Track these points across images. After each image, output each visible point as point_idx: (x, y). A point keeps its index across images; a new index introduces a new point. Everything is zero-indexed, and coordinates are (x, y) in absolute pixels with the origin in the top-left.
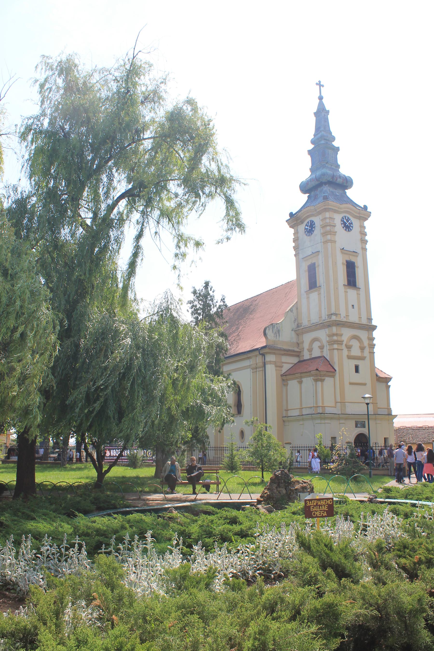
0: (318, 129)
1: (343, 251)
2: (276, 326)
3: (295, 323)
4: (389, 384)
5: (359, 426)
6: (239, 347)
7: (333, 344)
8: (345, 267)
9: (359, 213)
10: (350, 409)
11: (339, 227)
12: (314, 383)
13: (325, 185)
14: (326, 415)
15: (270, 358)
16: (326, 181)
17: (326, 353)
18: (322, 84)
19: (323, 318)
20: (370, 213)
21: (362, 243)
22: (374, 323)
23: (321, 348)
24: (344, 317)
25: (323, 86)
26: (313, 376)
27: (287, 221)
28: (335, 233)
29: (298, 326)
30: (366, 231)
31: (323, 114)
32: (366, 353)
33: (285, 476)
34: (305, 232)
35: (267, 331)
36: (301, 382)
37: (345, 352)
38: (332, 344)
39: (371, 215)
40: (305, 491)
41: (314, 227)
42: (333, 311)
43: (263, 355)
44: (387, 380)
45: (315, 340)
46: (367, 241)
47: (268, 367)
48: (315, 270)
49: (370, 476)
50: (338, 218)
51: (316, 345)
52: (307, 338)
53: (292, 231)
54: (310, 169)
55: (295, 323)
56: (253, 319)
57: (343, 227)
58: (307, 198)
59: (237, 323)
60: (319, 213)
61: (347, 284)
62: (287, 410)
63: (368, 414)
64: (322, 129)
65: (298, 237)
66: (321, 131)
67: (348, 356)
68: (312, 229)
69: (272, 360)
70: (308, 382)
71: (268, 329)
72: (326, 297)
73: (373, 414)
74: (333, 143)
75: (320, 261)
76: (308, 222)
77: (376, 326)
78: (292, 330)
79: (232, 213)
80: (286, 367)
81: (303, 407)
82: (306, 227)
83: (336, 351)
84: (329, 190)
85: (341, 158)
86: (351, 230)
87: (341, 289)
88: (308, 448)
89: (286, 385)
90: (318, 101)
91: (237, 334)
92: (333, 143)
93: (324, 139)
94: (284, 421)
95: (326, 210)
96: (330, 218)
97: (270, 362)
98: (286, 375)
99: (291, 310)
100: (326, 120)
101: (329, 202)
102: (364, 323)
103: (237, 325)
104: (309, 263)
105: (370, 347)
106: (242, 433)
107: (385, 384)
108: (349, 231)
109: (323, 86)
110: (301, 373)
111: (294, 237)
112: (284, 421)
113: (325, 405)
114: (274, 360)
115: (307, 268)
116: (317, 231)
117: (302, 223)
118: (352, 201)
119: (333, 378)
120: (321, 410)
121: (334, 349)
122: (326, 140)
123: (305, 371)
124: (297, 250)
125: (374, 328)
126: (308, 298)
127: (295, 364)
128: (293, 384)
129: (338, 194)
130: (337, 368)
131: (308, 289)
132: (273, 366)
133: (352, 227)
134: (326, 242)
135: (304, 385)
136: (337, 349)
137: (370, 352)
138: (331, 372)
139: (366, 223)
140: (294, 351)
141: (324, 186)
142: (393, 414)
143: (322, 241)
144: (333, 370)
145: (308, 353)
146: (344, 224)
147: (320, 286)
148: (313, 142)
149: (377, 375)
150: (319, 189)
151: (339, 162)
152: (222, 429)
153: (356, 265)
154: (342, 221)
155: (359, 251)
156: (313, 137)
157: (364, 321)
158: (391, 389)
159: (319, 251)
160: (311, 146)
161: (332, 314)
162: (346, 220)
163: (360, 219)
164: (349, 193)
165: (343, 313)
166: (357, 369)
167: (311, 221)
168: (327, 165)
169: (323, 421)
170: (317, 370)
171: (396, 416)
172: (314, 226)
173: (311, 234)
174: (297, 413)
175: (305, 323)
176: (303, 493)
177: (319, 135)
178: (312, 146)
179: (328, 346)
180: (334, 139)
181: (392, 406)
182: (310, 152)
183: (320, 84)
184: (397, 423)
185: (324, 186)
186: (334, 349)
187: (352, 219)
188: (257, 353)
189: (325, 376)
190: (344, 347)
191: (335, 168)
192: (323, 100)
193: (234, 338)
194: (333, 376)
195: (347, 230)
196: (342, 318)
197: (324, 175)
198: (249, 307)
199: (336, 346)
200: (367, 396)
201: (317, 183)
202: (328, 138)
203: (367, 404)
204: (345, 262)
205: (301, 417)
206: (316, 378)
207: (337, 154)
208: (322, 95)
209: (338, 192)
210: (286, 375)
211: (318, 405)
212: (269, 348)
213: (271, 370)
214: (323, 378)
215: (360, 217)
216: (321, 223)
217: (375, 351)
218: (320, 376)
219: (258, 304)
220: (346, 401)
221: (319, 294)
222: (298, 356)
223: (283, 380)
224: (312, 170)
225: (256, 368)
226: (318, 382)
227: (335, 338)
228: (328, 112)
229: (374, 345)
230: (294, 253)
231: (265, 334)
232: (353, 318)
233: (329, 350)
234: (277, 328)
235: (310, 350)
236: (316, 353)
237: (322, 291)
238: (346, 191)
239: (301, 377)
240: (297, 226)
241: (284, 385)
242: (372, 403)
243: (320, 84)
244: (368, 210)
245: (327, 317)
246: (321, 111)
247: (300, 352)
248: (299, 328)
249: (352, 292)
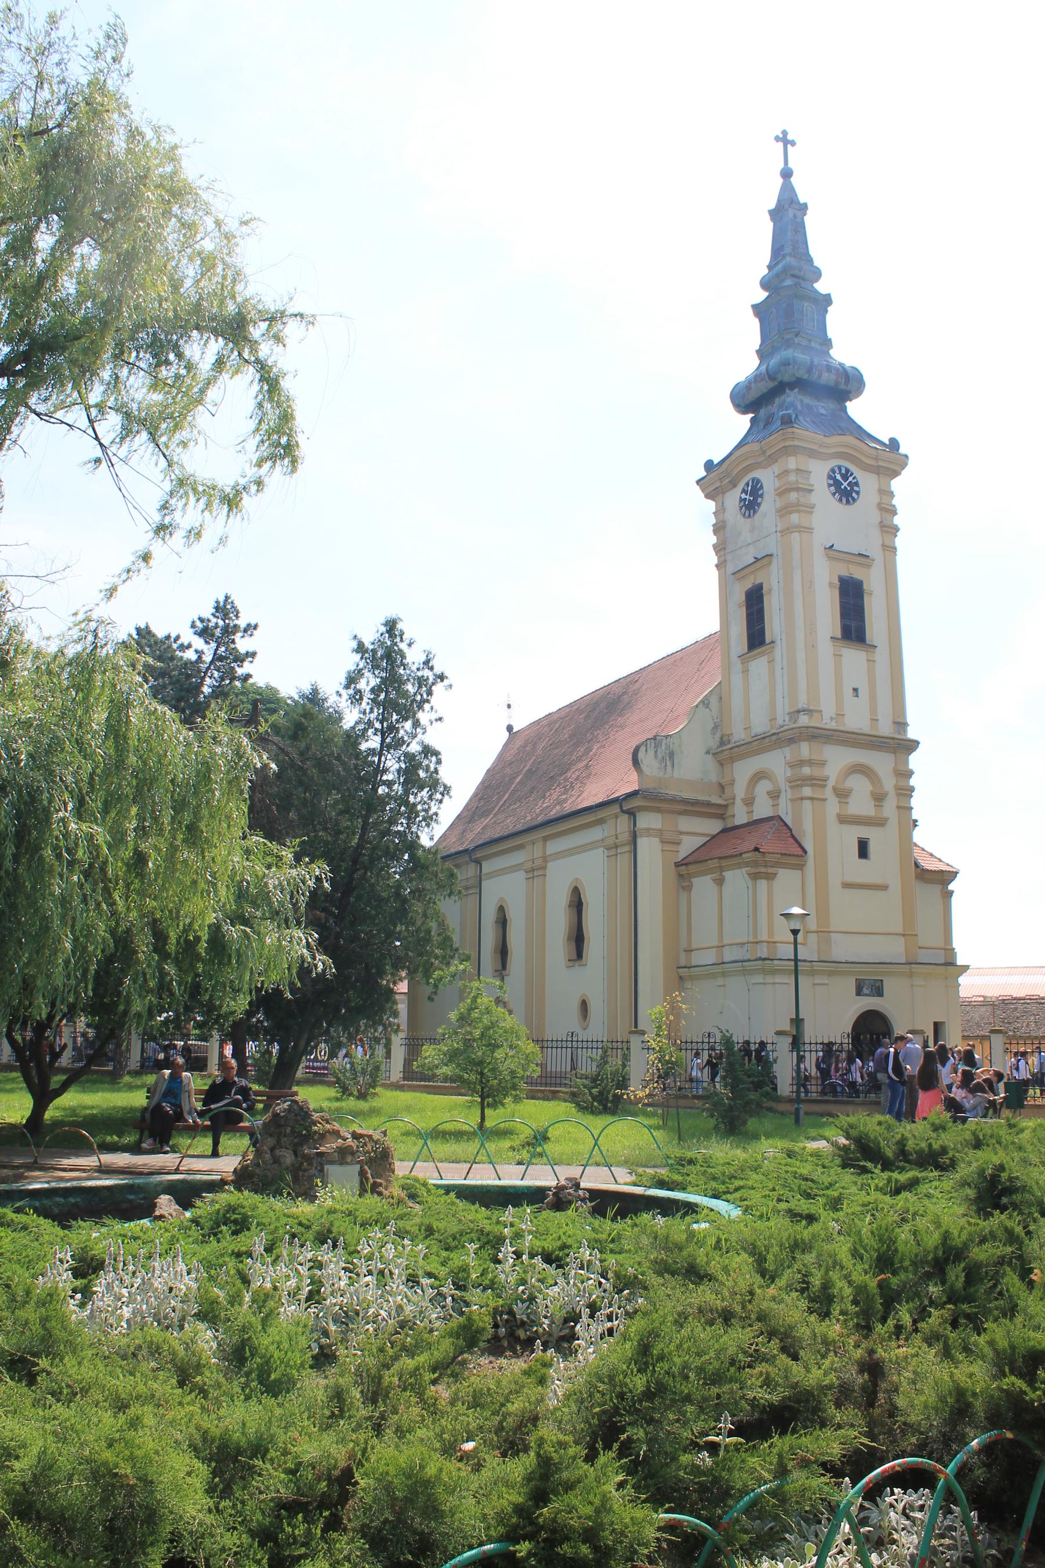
0: (777, 251)
1: (830, 553)
2: (664, 742)
3: (714, 734)
4: (951, 887)
5: (865, 991)
6: (584, 795)
7: (802, 786)
8: (837, 593)
9: (876, 459)
10: (843, 949)
11: (822, 495)
12: (750, 883)
13: (792, 389)
14: (775, 962)
15: (645, 821)
16: (793, 379)
17: (785, 810)
18: (789, 137)
19: (780, 722)
20: (906, 456)
21: (882, 532)
22: (912, 734)
23: (774, 795)
24: (831, 719)
25: (793, 144)
26: (747, 864)
27: (698, 482)
28: (810, 509)
29: (722, 743)
30: (894, 502)
31: (791, 213)
32: (889, 808)
33: (296, 1115)
34: (741, 508)
35: (641, 755)
36: (720, 882)
37: (833, 807)
38: (798, 786)
39: (910, 462)
40: (349, 1159)
41: (761, 496)
42: (802, 703)
43: (632, 814)
44: (943, 878)
45: (760, 776)
46: (896, 529)
47: (643, 843)
48: (762, 602)
49: (797, 1121)
50: (819, 472)
51: (763, 788)
52: (743, 771)
53: (711, 505)
54: (757, 352)
55: (714, 734)
56: (622, 727)
57: (834, 494)
58: (748, 425)
59: (589, 736)
60: (772, 459)
61: (839, 635)
62: (689, 951)
63: (796, 960)
64: (788, 250)
65: (724, 522)
66: (784, 256)
67: (839, 816)
68: (755, 499)
69: (652, 827)
70: (736, 879)
71: (643, 748)
72: (785, 668)
73: (903, 961)
74: (815, 285)
75: (773, 581)
76: (747, 484)
77: (917, 743)
78: (708, 752)
79: (272, 414)
80: (688, 845)
81: (725, 942)
82: (743, 496)
83: (807, 805)
84: (802, 401)
85: (835, 323)
86: (854, 500)
87: (825, 648)
88: (600, 1045)
89: (689, 888)
90: (780, 181)
91: (585, 763)
92: (815, 285)
93: (793, 276)
94: (680, 977)
95: (787, 451)
96: (798, 470)
97: (648, 832)
98: (686, 864)
99: (705, 703)
100: (800, 229)
101: (795, 430)
102: (886, 734)
103: (589, 742)
104: (748, 584)
105: (898, 795)
106: (584, 1005)
107: (941, 887)
108: (848, 502)
109: (793, 144)
110: (720, 858)
111: (714, 521)
112: (680, 977)
113: (776, 939)
114: (659, 826)
115: (743, 598)
116: (768, 504)
117: (735, 486)
118: (859, 427)
119: (798, 873)
120: (765, 950)
121: (802, 799)
122: (798, 277)
123: (731, 852)
124: (722, 553)
125: (912, 746)
126: (746, 671)
127: (714, 837)
128: (703, 885)
129: (823, 411)
130: (809, 846)
131: (746, 650)
132: (656, 841)
133: (858, 493)
134: (787, 531)
135: (727, 888)
136: (811, 799)
137: (898, 807)
138: (794, 855)
139: (896, 484)
140: (708, 804)
141: (788, 391)
142: (959, 963)
143: (779, 529)
144: (800, 852)
145: (745, 809)
146: (837, 484)
147: (773, 642)
148: (765, 284)
149: (917, 865)
150: (777, 401)
151: (831, 333)
152: (435, 993)
153: (865, 587)
154: (829, 477)
155: (875, 552)
156: (766, 271)
157: (885, 729)
158: (955, 900)
159: (771, 555)
160: (762, 295)
161: (799, 711)
162: (842, 475)
163: (878, 474)
164: (855, 409)
165: (828, 708)
166: (863, 849)
167: (753, 480)
168: (796, 340)
169: (769, 979)
170: (756, 849)
171: (966, 968)
172: (760, 492)
173: (755, 512)
174: (708, 957)
175: (739, 734)
176: (341, 1164)
177: (780, 267)
178: (765, 294)
179: (789, 790)
180: (817, 274)
181: (957, 943)
182: (758, 310)
183: (785, 140)
184: (969, 987)
185: (788, 391)
186: (802, 799)
187: (858, 474)
188: (615, 809)
190: (828, 793)
191: (818, 347)
192: (792, 179)
193: (577, 773)
194: (801, 867)
195: (844, 500)
196: (827, 720)
197: (786, 363)
198: (619, 697)
199: (807, 791)
200: (796, 910)
201: (771, 385)
202: (802, 274)
203: (795, 932)
205: (721, 969)
206: (753, 870)
207: (826, 311)
208: (790, 165)
209: (824, 407)
210: (686, 864)
211: (759, 939)
212: (645, 797)
213: (649, 849)
214: (771, 870)
215: (879, 467)
216: (777, 485)
217: (912, 805)
218: (766, 866)
219: (639, 689)
221: (771, 661)
222: (721, 817)
223: (681, 876)
224: (761, 353)
225: (616, 847)
226: (758, 882)
227: (806, 770)
228: (804, 208)
229: (912, 789)
230: (715, 560)
231: (636, 762)
232: (856, 720)
233: (792, 800)
234: (668, 747)
235: (749, 802)
236: (763, 809)
237: (779, 652)
238: (848, 404)
239: (721, 869)
240: (723, 493)
241: (683, 888)
242: (904, 935)
243: (785, 140)
244: (902, 451)
245: (787, 718)
246: (786, 207)
247: (726, 806)
248: (725, 748)
249: (853, 656)
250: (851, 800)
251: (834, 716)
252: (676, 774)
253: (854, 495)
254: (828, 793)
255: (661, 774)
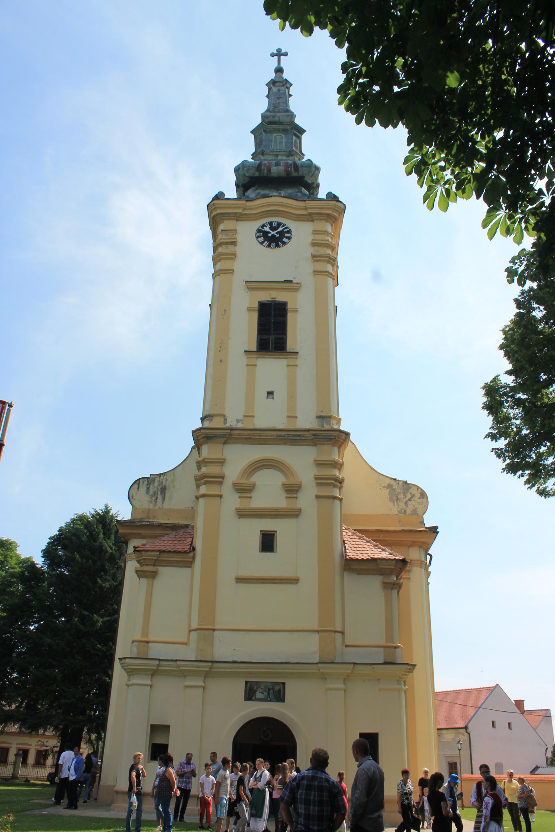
5: (259, 695)
8: (256, 315)
61: (255, 349)
108: (277, 246)
153: (289, 306)
189: (156, 563)
195: (273, 245)
204: (256, 305)
215: (310, 214)
220: (217, 627)
234: (160, 483)
250: (253, 494)
251: (241, 417)
252: (166, 505)
253: (285, 240)
254: (227, 490)
255: (151, 506)
